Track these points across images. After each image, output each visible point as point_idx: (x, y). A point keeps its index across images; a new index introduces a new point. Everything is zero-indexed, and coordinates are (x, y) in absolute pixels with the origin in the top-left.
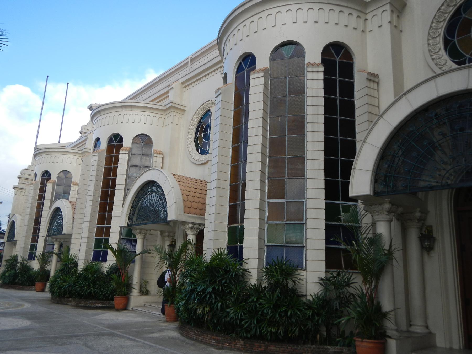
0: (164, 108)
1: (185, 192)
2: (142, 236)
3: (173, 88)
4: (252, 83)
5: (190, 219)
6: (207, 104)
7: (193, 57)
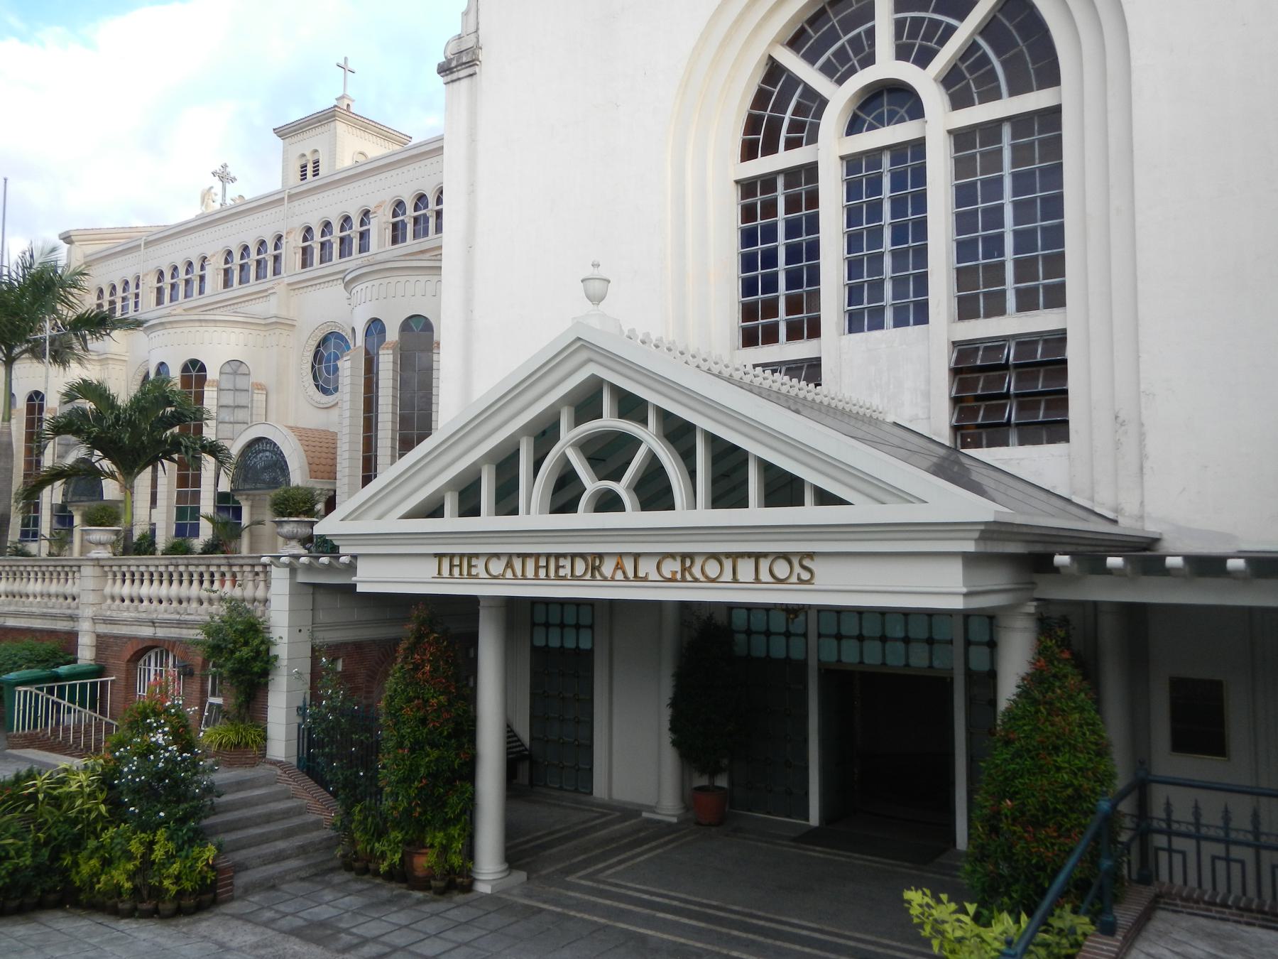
0: (263, 322)
1: (309, 453)
2: (249, 503)
3: (274, 293)
4: (381, 358)
5: (318, 485)
6: (329, 326)
7: (293, 191)
